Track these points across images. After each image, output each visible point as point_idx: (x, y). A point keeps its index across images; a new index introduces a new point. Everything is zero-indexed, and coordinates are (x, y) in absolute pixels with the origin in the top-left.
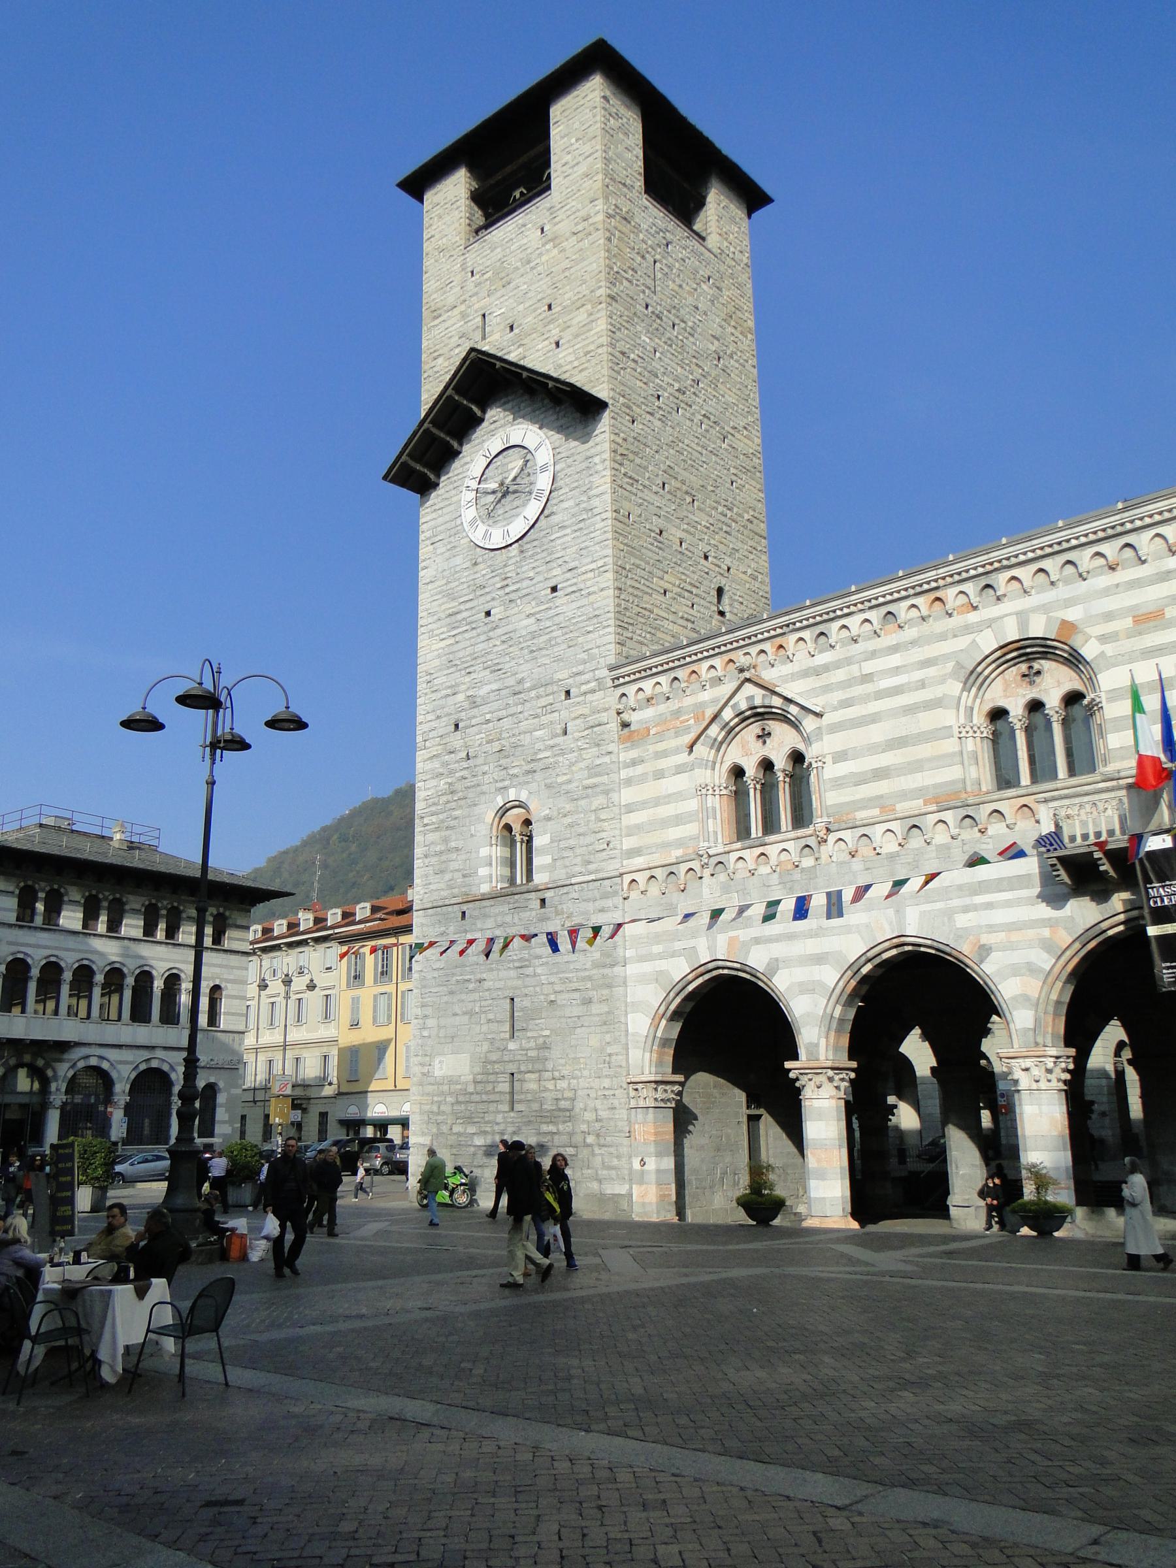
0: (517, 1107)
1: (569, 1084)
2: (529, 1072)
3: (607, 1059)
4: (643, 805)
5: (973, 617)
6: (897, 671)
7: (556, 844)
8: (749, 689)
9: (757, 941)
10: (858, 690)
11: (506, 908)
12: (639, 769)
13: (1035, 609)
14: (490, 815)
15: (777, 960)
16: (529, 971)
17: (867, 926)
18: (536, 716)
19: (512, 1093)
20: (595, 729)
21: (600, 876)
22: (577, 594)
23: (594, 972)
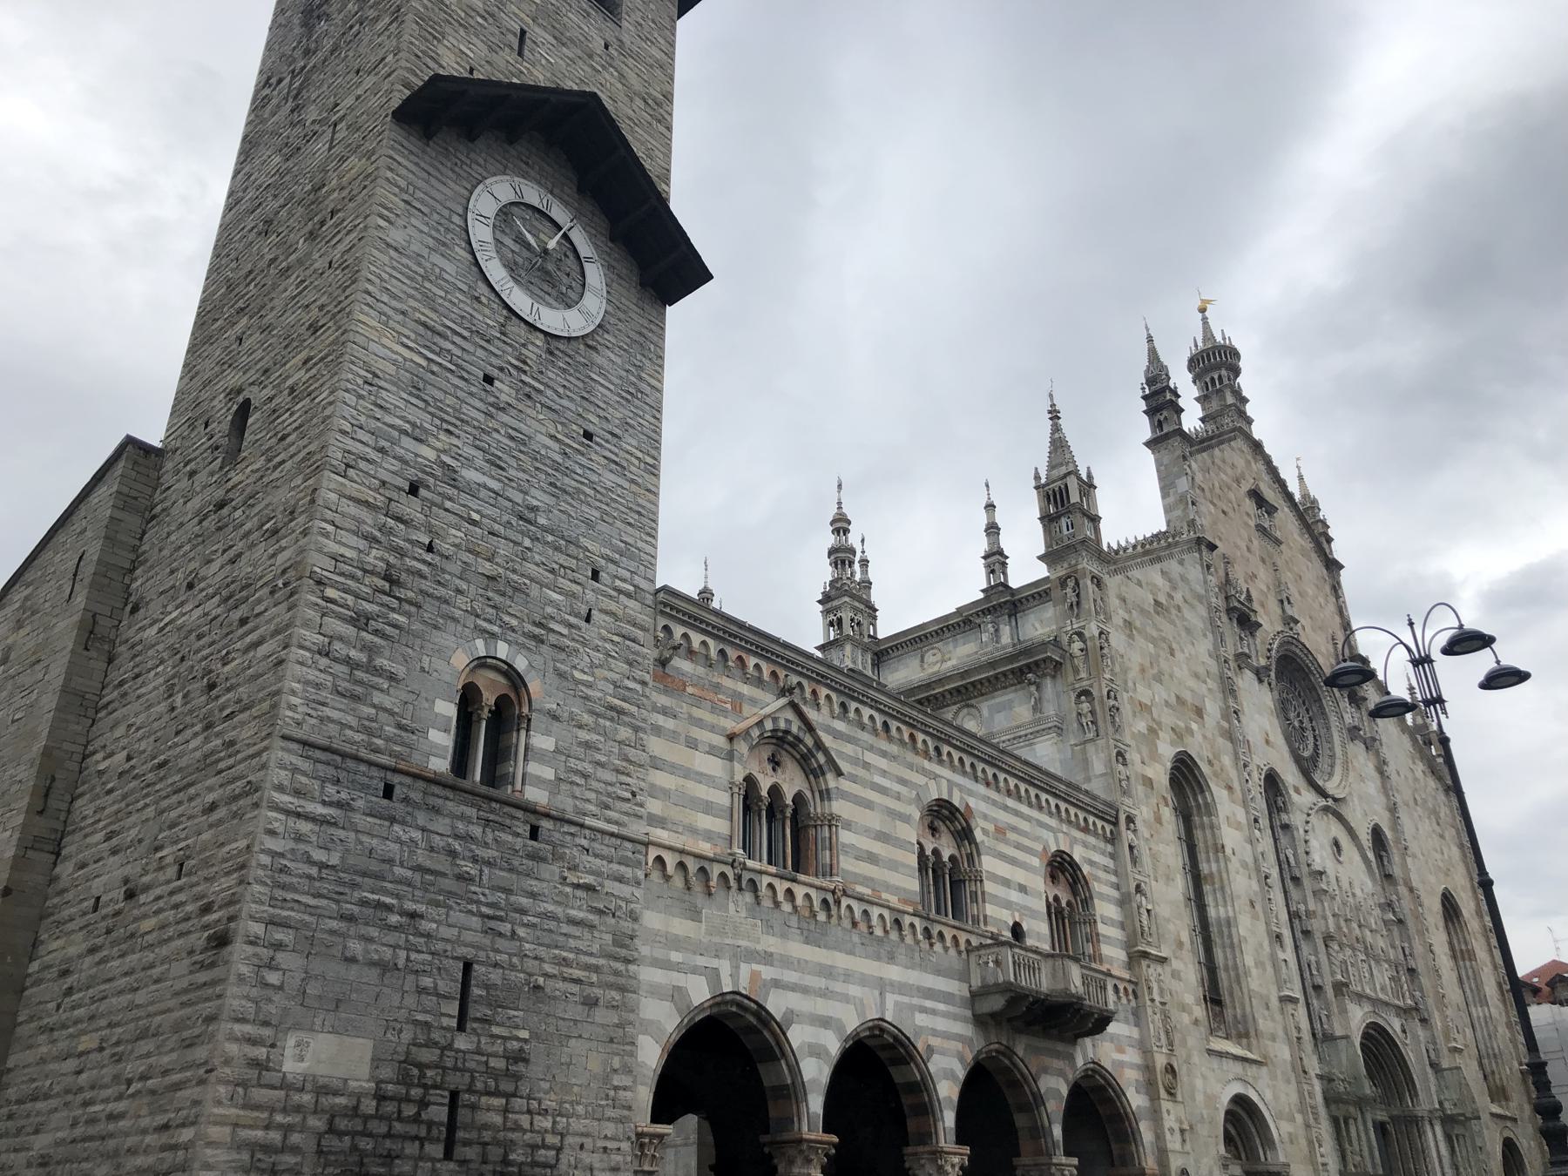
0: (461, 1152)
1: (554, 1122)
2: (489, 1094)
3: (612, 1093)
4: (673, 769)
5: (926, 764)
6: (884, 773)
7: (563, 758)
8: (790, 714)
9: (776, 984)
10: (861, 772)
11: (471, 812)
12: (669, 724)
13: (958, 785)
14: (461, 660)
16: (506, 928)
17: (861, 1000)
18: (552, 571)
19: (452, 1125)
20: (627, 642)
21: (624, 831)
23: (602, 962)
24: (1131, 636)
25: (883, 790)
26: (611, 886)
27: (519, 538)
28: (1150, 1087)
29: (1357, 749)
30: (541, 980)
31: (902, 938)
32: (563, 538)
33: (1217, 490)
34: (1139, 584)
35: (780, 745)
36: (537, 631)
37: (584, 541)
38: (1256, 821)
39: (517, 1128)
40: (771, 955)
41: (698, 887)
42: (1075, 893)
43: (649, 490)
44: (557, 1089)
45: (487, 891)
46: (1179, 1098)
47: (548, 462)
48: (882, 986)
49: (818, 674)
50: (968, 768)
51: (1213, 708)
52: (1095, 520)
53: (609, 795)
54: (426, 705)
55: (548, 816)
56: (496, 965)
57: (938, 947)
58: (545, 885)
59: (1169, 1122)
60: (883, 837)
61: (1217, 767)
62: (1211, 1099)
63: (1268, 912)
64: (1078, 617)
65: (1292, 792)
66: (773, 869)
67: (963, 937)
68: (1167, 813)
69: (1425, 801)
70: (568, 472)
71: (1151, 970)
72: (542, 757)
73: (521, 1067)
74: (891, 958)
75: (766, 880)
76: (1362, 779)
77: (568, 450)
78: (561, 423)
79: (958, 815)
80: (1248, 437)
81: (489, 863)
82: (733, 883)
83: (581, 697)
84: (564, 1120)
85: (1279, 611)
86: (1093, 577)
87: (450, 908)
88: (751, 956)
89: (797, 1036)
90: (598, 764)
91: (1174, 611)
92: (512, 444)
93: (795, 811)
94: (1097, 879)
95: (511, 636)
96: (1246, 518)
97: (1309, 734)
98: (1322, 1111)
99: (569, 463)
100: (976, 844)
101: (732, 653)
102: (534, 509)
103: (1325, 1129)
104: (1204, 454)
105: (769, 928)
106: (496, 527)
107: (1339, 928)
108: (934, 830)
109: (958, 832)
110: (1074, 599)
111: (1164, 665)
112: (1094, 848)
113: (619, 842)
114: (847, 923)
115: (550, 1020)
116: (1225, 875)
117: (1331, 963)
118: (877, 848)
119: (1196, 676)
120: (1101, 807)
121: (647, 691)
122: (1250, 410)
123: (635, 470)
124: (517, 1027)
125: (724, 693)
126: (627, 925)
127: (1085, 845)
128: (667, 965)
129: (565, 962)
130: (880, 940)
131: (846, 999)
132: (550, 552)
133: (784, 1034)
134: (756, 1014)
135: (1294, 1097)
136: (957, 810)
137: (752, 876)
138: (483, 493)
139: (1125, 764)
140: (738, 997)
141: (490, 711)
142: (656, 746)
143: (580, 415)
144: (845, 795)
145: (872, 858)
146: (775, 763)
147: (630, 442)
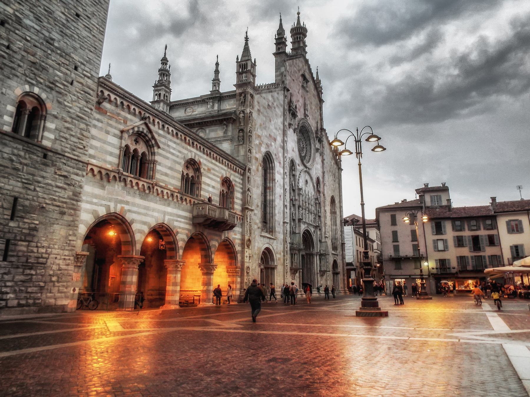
4: (100, 140)
5: (189, 147)
6: (174, 149)
8: (144, 127)
9: (129, 211)
10: (166, 147)
11: (20, 147)
12: (100, 125)
13: (197, 154)
14: (19, 91)
15: (134, 219)
16: (32, 187)
17: (157, 217)
18: (59, 64)
20: (87, 94)
21: (79, 159)
22: (89, 30)
23: (68, 201)
24: (259, 114)
25: (173, 154)
26: (73, 177)
27: (46, 49)
28: (242, 245)
29: (318, 155)
30: (44, 205)
31: (173, 200)
32: (64, 52)
33: (293, 73)
34: (264, 98)
35: (139, 136)
36: (51, 85)
37: (73, 55)
38: (286, 173)
39: (32, 252)
40: (129, 202)
41: (105, 179)
42: (229, 189)
43: (100, 40)
44: (48, 240)
45: (25, 175)
46: (250, 248)
47: (60, 22)
48: (165, 213)
49: (156, 114)
50: (202, 150)
51: (279, 139)
52: (254, 76)
53: (75, 146)
54: (3, 106)
55: (51, 151)
56: (27, 199)
57: (184, 203)
58: (48, 174)
59: (246, 254)
60: (171, 168)
61: (277, 156)
62: (259, 248)
63: (284, 199)
64: (244, 106)
65: (297, 165)
66: (132, 176)
67: (193, 200)
68: (260, 168)
69: (332, 171)
70: (68, 28)
71: (248, 213)
72: (50, 130)
73: (35, 233)
74: (169, 205)
75: (129, 179)
76: (317, 164)
77: (69, 19)
78: (67, 9)
79: (196, 164)
80: (304, 57)
81: (26, 165)
82: (118, 179)
83: (67, 111)
84: (50, 250)
85: (303, 112)
86: (251, 94)
87: (9, 179)
88: (121, 202)
89: (135, 227)
90: (72, 135)
91: (273, 108)
92: (46, 13)
93: (142, 158)
94: (237, 186)
95: (40, 86)
96: (299, 83)
97: (305, 149)
98: (289, 252)
99: (69, 25)
100: (201, 173)
101: (126, 103)
102: (53, 40)
103: (288, 257)
104: (291, 61)
105: (129, 193)
106: (37, 44)
107: (303, 204)
108: (187, 167)
109: (195, 169)
110: (243, 101)
111: (267, 125)
112: (237, 177)
113: (77, 162)
114: (155, 194)
115: (47, 218)
116: (274, 188)
117: (299, 214)
118: (169, 172)
119: (276, 129)
120: (241, 165)
121: (93, 113)
122: (307, 49)
123: (95, 32)
124: (34, 220)
125: (121, 117)
126: (78, 189)
127: (234, 176)
128: (91, 203)
129: (54, 200)
130: (166, 200)
131: (152, 216)
132: (58, 57)
133: (130, 226)
134: (121, 220)
135: (282, 248)
136: (196, 162)
137: (125, 177)
138: (32, 30)
139: (251, 153)
140: (116, 214)
141: (30, 112)
142: (94, 131)
143: (75, 7)
144: (160, 155)
145: (166, 175)
146: (136, 142)
147: (94, 21)
